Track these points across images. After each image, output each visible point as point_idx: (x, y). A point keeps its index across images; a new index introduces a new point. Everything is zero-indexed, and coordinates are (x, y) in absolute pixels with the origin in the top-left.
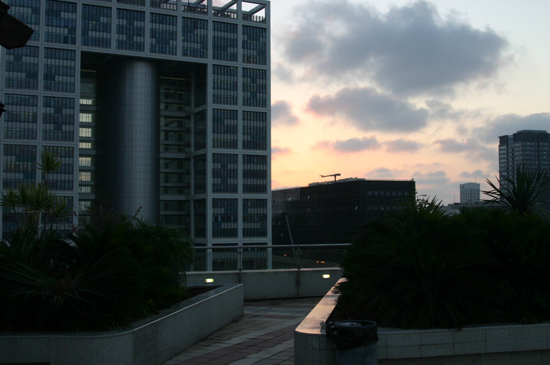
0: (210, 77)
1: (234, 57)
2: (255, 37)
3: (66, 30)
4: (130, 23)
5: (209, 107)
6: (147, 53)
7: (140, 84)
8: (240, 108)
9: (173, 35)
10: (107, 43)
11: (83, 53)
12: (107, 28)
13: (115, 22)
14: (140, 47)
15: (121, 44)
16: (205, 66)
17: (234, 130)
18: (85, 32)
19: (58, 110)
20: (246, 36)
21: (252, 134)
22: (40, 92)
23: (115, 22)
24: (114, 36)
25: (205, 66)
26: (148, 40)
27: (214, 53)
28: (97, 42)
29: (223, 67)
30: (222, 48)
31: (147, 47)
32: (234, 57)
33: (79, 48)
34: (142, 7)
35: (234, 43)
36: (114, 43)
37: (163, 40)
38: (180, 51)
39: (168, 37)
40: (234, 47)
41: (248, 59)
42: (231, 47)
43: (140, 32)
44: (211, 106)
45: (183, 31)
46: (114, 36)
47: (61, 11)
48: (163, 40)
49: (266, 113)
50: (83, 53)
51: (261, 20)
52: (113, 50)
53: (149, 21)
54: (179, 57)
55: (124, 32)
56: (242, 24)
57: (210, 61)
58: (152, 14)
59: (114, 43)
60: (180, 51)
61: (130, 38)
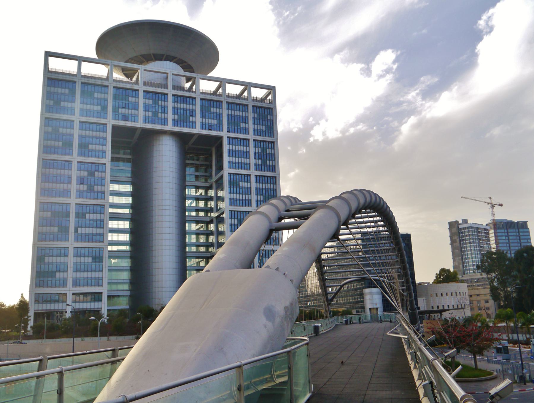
0: (226, 147)
1: (247, 131)
2: (263, 115)
3: (99, 108)
4: (156, 102)
5: (225, 171)
6: (170, 127)
7: (166, 157)
8: (253, 172)
9: (192, 113)
10: (135, 118)
11: (114, 127)
12: (135, 107)
13: (141, 101)
14: (164, 121)
15: (146, 120)
16: (220, 138)
17: (248, 191)
18: (115, 110)
19: (91, 174)
20: (256, 114)
21: (264, 194)
22: (75, 158)
23: (141, 101)
24: (141, 112)
25: (220, 138)
26: (170, 116)
27: (228, 128)
28: (125, 118)
29: (236, 140)
31: (170, 122)
32: (247, 131)
33: (110, 121)
34: (166, 90)
35: (245, 120)
36: (141, 118)
37: (184, 118)
38: (198, 125)
39: (188, 114)
40: (245, 123)
42: (243, 122)
43: (164, 110)
44: (227, 170)
45: (202, 111)
46: (141, 112)
47: (94, 92)
49: (275, 177)
50: (114, 127)
51: (268, 102)
52: (140, 124)
53: (171, 100)
54: (198, 130)
56: (251, 104)
57: (225, 134)
58: (174, 95)
59: (141, 118)
60: (198, 125)
61: (156, 114)
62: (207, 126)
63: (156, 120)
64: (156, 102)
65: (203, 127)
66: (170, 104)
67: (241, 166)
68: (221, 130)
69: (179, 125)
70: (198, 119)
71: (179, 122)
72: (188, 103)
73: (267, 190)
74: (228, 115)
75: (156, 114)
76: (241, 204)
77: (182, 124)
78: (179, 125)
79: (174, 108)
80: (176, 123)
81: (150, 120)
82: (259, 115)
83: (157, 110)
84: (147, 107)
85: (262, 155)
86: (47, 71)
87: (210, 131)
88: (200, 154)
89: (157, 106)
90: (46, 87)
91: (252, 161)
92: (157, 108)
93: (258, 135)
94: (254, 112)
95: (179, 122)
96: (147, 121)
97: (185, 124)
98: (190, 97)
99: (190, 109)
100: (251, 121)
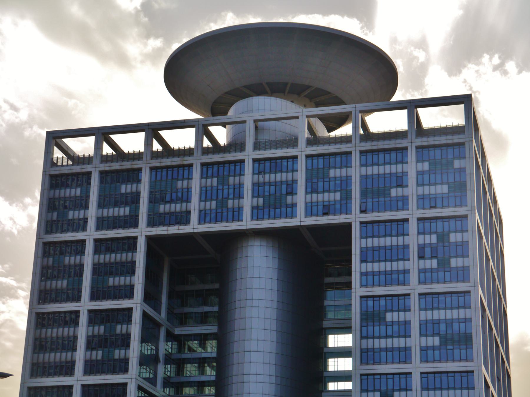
6: (247, 223)
11: (150, 239)
14: (237, 215)
15: (203, 218)
16: (348, 227)
24: (195, 206)
25: (348, 227)
26: (247, 202)
30: (376, 192)
31: (247, 213)
35: (400, 181)
38: (301, 210)
39: (284, 191)
41: (425, 201)
45: (309, 179)
48: (275, 200)
50: (150, 239)
52: (194, 226)
54: (300, 219)
55: (214, 197)
57: (355, 218)
60: (301, 210)
62: (320, 207)
63: (225, 214)
64: (223, 181)
65: (310, 211)
66: (248, 180)
67: (390, 278)
68: (347, 211)
69: (266, 216)
70: (301, 198)
71: (266, 210)
72: (284, 169)
73: (449, 323)
74: (364, 178)
75: (222, 203)
76: (390, 360)
77: (272, 213)
78: (266, 216)
79: (256, 185)
80: (257, 213)
81: (213, 215)
82: (433, 163)
83: (225, 195)
84: (209, 193)
85: (440, 248)
86: (49, 165)
87: (325, 217)
88: (315, 264)
89: (226, 187)
90: (46, 191)
91: (413, 264)
92: (226, 191)
93: (431, 208)
94: (419, 159)
95: (266, 210)
96: (208, 219)
97: (278, 210)
98: (287, 158)
99: (287, 181)
100: (412, 180)
